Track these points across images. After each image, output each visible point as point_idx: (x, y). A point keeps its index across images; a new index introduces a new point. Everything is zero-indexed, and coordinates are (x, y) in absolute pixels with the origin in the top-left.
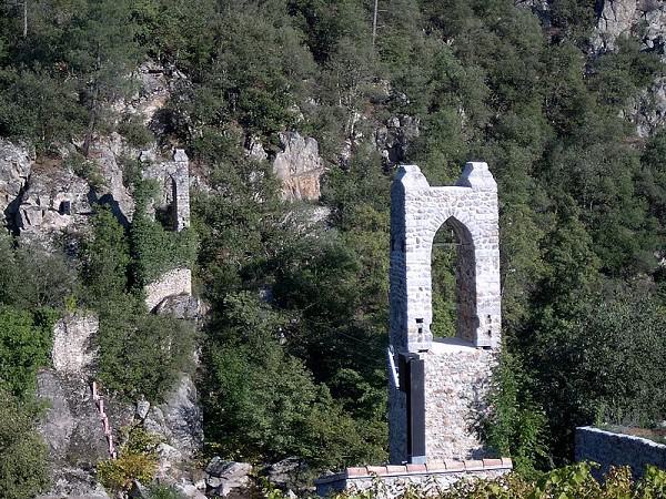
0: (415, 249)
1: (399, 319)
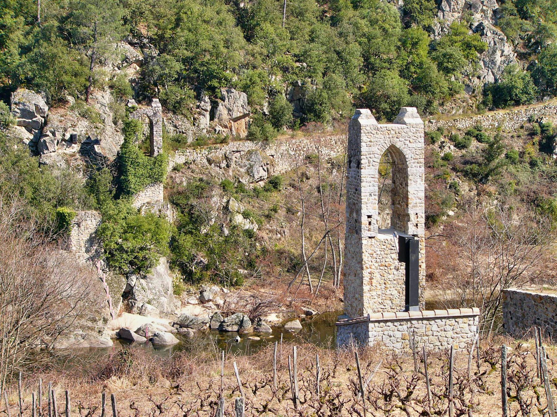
0: (367, 167)
1: (355, 215)
